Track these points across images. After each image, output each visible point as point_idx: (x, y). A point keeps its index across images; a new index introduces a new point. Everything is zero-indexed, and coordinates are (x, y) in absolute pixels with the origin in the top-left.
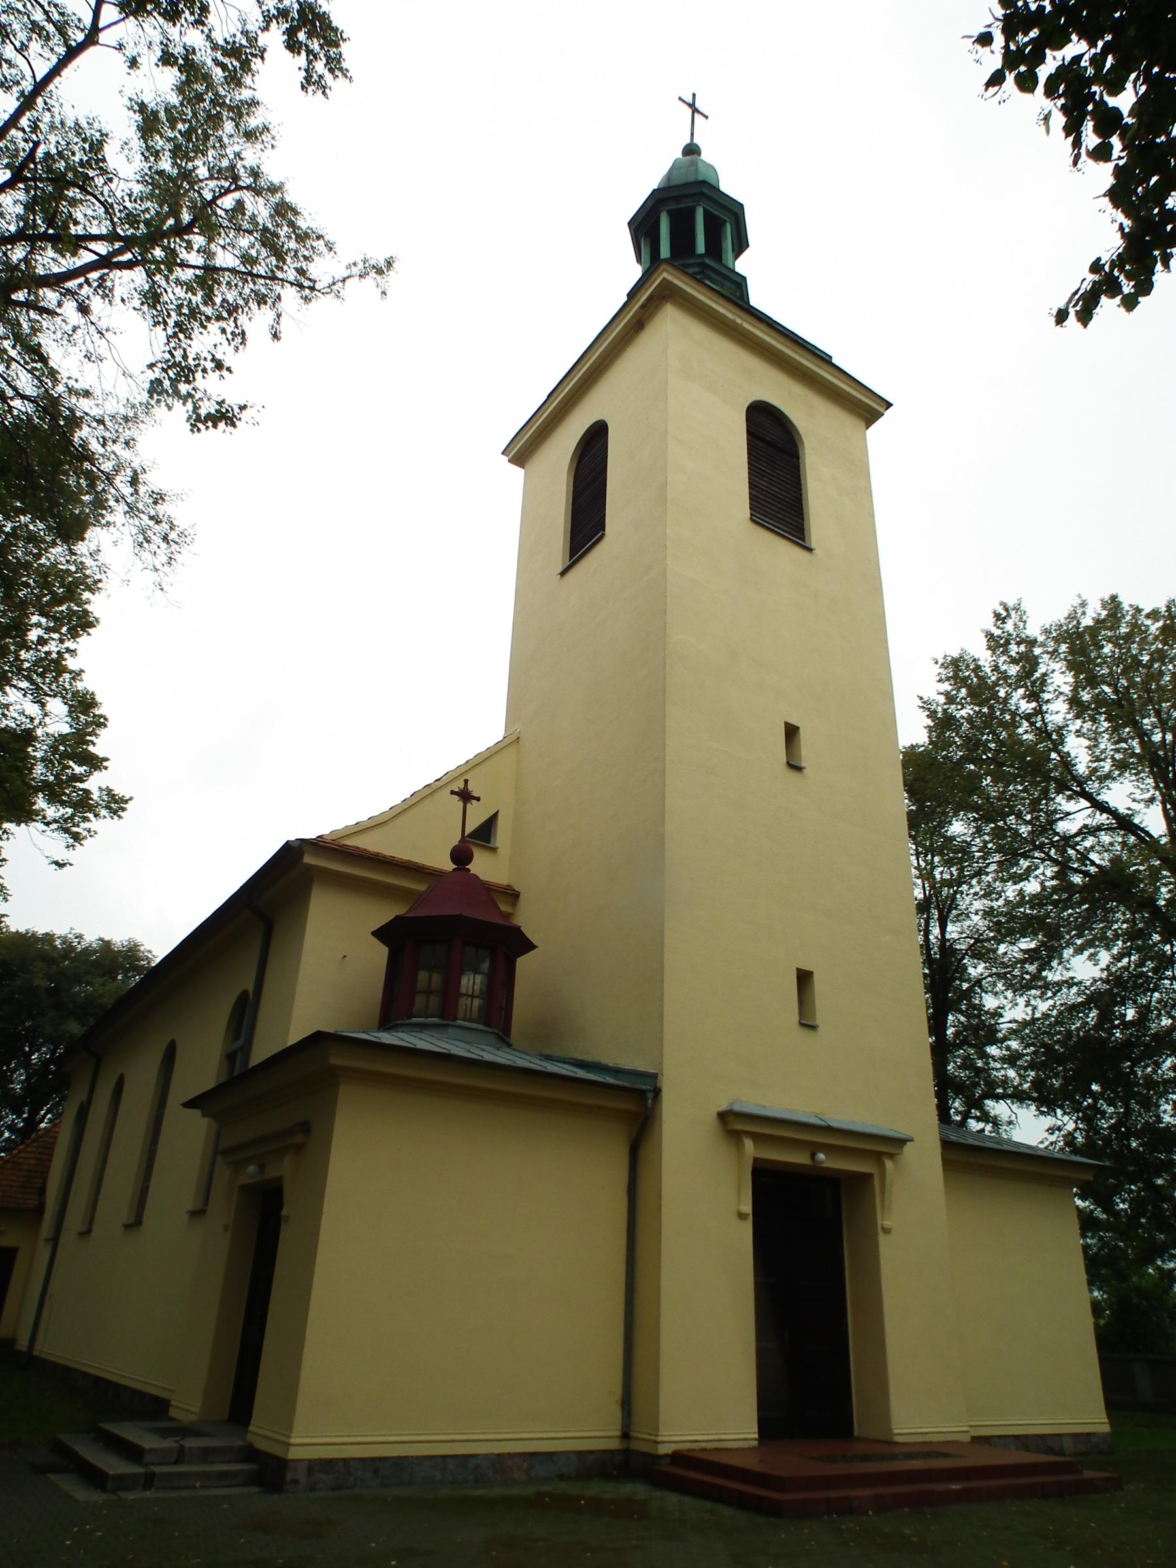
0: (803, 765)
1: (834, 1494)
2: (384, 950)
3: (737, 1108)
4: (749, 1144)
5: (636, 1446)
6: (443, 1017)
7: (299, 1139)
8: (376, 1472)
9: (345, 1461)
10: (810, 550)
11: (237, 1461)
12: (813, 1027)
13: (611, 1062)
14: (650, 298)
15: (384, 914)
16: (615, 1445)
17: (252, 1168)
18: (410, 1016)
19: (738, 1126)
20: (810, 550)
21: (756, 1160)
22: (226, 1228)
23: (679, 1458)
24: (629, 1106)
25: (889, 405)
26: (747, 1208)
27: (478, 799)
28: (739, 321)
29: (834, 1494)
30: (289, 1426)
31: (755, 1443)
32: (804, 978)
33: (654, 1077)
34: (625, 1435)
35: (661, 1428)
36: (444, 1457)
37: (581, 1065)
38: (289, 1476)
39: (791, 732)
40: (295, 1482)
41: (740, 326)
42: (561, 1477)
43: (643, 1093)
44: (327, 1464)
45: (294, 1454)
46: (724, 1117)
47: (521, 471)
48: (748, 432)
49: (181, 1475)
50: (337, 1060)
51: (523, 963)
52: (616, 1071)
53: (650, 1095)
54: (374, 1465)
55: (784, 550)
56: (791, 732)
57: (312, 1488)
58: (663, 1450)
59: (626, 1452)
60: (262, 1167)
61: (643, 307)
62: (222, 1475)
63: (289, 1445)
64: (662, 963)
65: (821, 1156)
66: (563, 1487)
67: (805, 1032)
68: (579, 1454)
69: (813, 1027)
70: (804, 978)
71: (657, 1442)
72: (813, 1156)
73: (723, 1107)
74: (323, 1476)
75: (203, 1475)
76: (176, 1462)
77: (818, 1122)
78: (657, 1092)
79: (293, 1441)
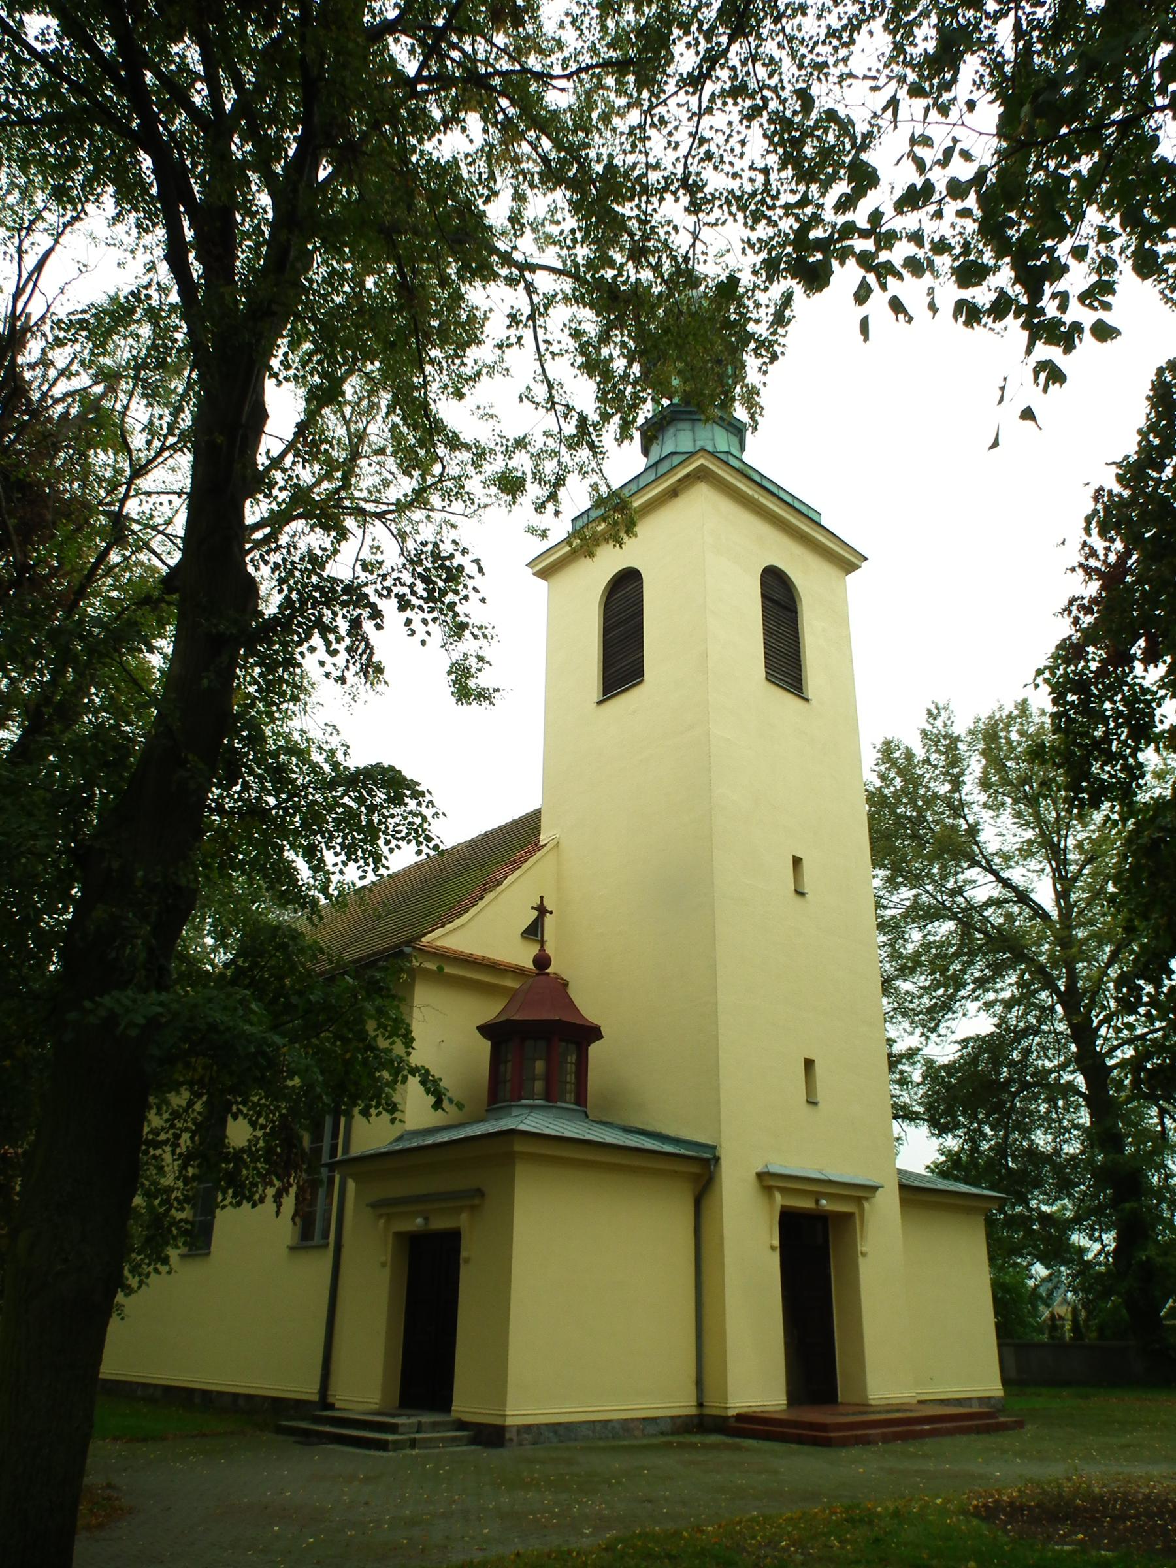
0: (806, 891)
1: (859, 1432)
2: (487, 1045)
3: (774, 1169)
4: (778, 1196)
5: (707, 1411)
6: (547, 1098)
7: (476, 1202)
8: (555, 1432)
9: (538, 1426)
10: (807, 700)
11: (457, 1430)
12: (815, 1104)
13: (671, 1132)
14: (688, 475)
15: (490, 1010)
16: (693, 1411)
17: (419, 1221)
18: (520, 1099)
19: (772, 1183)
20: (807, 700)
21: (783, 1207)
22: (383, 1265)
23: (740, 1417)
24: (695, 1169)
25: (866, 559)
26: (776, 1243)
27: (551, 912)
28: (756, 496)
29: (859, 1432)
30: (503, 1403)
31: (784, 1407)
32: (809, 1064)
33: (714, 1148)
34: (700, 1405)
35: (729, 1397)
36: (594, 1422)
37: (628, 1130)
38: (508, 1436)
39: (797, 862)
40: (511, 1440)
41: (757, 500)
42: (662, 1434)
43: (707, 1161)
44: (528, 1428)
45: (509, 1422)
46: (760, 1176)
47: (546, 583)
48: (763, 595)
49: (430, 1439)
50: (518, 1147)
51: (594, 1049)
52: (677, 1141)
53: (713, 1162)
54: (554, 1427)
55: (789, 701)
56: (797, 862)
57: (520, 1444)
58: (732, 1413)
59: (701, 1417)
60: (426, 1219)
61: (679, 480)
62: (454, 1439)
63: (505, 1416)
64: (718, 1062)
65: (823, 1202)
66: (664, 1439)
67: (811, 1107)
68: (672, 1418)
69: (815, 1104)
70: (809, 1064)
71: (727, 1408)
72: (817, 1202)
73: (759, 1170)
74: (526, 1436)
75: (442, 1439)
76: (418, 1432)
77: (822, 1177)
78: (717, 1160)
79: (508, 1413)
